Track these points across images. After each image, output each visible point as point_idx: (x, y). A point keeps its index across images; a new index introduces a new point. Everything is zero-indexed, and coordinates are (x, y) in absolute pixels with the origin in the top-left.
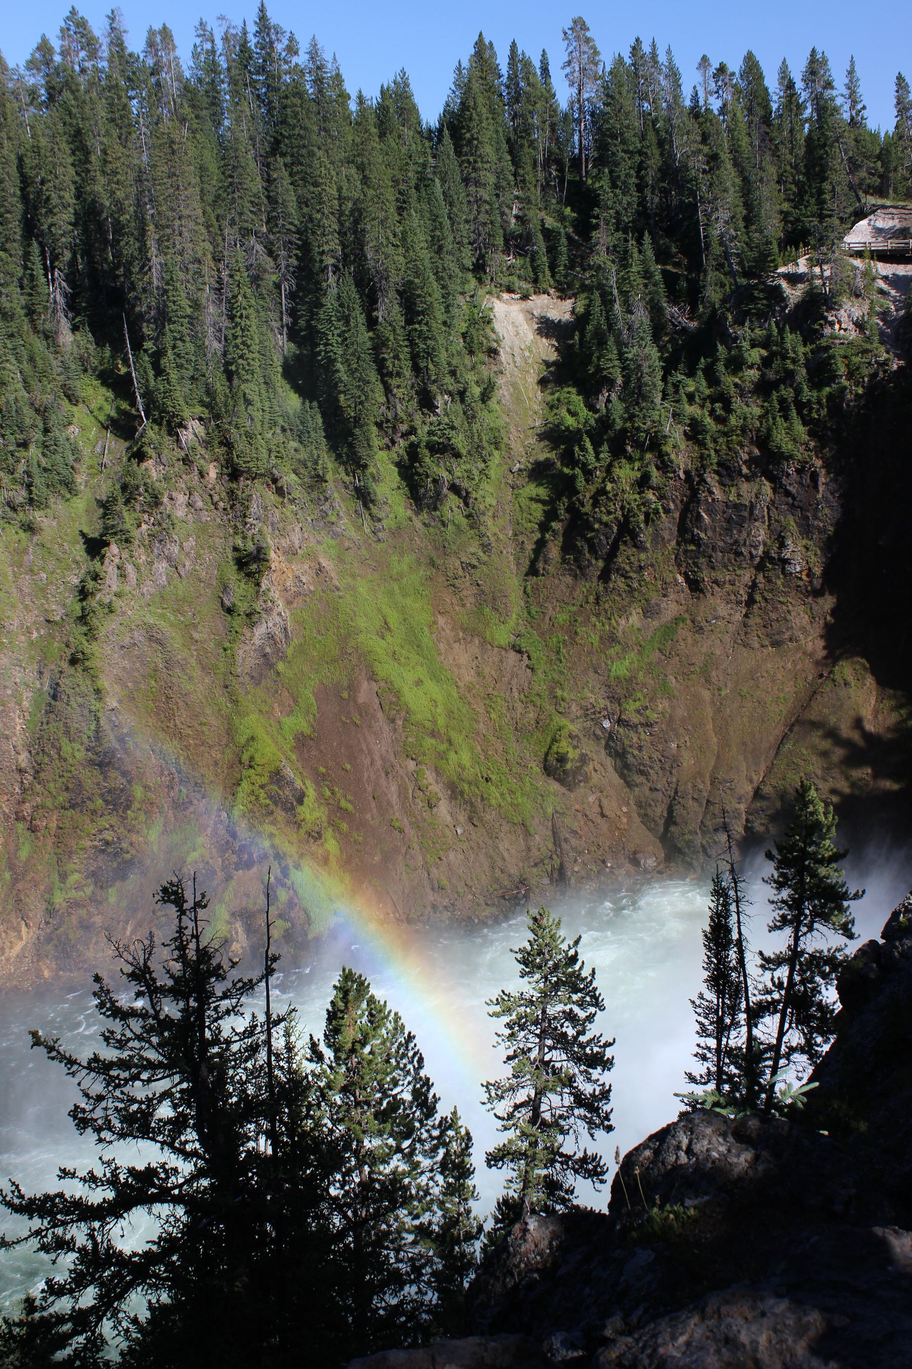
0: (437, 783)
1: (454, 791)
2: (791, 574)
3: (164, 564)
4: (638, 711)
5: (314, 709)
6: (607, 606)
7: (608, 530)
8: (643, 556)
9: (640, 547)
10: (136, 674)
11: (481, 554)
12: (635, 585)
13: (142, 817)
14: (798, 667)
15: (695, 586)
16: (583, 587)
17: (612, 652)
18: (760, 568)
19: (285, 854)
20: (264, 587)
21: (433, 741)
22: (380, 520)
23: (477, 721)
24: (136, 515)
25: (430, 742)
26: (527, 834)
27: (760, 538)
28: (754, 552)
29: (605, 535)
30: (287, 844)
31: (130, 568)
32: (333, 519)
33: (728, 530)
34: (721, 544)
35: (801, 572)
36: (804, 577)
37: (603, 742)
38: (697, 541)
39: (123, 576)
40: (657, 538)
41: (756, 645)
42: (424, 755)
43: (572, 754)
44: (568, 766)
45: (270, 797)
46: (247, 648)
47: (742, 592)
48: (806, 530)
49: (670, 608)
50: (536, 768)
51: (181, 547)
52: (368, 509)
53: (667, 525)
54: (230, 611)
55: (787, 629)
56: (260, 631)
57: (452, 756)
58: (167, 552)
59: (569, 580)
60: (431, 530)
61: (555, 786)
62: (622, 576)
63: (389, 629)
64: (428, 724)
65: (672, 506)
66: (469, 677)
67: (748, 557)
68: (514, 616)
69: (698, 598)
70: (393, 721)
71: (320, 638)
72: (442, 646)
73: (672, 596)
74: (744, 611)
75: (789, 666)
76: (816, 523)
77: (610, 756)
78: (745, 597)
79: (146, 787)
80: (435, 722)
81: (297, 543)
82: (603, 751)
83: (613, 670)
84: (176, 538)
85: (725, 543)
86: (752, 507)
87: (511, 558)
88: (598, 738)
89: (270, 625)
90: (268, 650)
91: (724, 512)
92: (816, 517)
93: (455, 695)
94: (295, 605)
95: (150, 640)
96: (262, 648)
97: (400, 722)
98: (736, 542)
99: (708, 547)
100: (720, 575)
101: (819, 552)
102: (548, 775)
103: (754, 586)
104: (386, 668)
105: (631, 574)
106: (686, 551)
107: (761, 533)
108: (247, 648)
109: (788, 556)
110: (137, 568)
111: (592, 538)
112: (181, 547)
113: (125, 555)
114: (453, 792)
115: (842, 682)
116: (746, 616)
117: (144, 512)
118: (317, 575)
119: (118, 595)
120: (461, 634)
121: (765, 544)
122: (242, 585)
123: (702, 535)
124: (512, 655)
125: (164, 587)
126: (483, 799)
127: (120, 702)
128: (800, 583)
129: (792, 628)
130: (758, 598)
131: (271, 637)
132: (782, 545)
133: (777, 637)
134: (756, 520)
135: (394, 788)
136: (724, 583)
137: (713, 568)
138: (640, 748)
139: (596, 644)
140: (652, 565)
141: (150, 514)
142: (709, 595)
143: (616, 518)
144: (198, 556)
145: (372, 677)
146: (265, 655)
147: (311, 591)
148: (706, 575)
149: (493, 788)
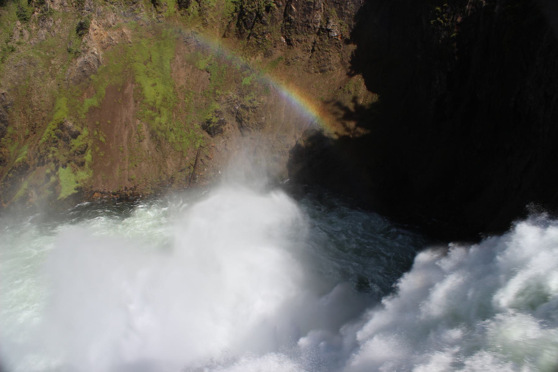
0: (147, 130)
1: (153, 134)
2: (332, 37)
3: (45, 31)
4: (250, 101)
5: (103, 96)
6: (246, 51)
7: (251, 15)
8: (265, 28)
9: (264, 23)
10: (20, 78)
11: (202, 28)
12: (260, 42)
13: (9, 141)
14: (331, 83)
15: (289, 42)
16: (241, 42)
17: (245, 73)
18: (318, 34)
19: (58, 161)
20: (84, 41)
21: (150, 112)
22: (160, 13)
23: (178, 104)
24: (32, 8)
25: (149, 112)
26: (182, 157)
27: (318, 19)
28: (316, 26)
29: (250, 18)
30: (61, 156)
31: (25, 32)
32: (137, 12)
33: (304, 15)
34: (301, 22)
35: (337, 36)
36: (339, 39)
37: (235, 115)
38: (289, 20)
39: (22, 35)
40: (273, 19)
41: (313, 72)
42: (144, 117)
43: (215, 120)
44: (211, 126)
45: (57, 135)
46: (73, 68)
47: (310, 46)
48: (341, 15)
49: (278, 53)
50: (197, 126)
51: (54, 23)
52: (156, 7)
53: (278, 12)
54: (69, 51)
55: (328, 64)
56: (80, 60)
57: (157, 119)
58: (46, 25)
59: (236, 39)
60: (184, 17)
61: (206, 134)
62: (255, 37)
63: (151, 61)
64: (151, 104)
65: (281, 3)
66: (183, 83)
67: (313, 28)
68: (210, 56)
69: (290, 48)
70: (136, 102)
71: (115, 64)
72: (174, 69)
73: (278, 47)
74: (310, 55)
75: (327, 82)
76: (346, 11)
77: (237, 121)
78: (311, 48)
79: (15, 128)
80: (154, 103)
81: (111, 22)
82: (235, 119)
83: (244, 81)
84: (52, 19)
85: (303, 21)
86: (315, 3)
87: (218, 30)
88: (233, 113)
89: (86, 58)
90: (85, 69)
91: (303, 6)
92: (346, 9)
93: (171, 91)
94: (107, 50)
95: (30, 63)
96: (81, 68)
97: (139, 103)
98: (308, 21)
99: (295, 23)
100: (300, 38)
101: (348, 27)
102: (204, 129)
103: (315, 43)
104: (141, 79)
105: (258, 36)
106: (285, 25)
107: (319, 17)
108: (73, 68)
109: (330, 28)
110: (30, 32)
111: (245, 20)
112: (54, 23)
113: (24, 26)
114: (152, 135)
115: (347, 92)
116: (310, 57)
117: (36, 7)
118: (121, 36)
119: (19, 44)
120: (185, 64)
121: (321, 22)
122: (77, 40)
123: (292, 18)
124: (205, 73)
125: (43, 40)
126: (166, 139)
127: (9, 90)
128: (337, 42)
129: (331, 63)
130: (316, 48)
131: (87, 63)
132: (328, 23)
133: (323, 68)
134: (317, 10)
135: (127, 132)
136: (302, 41)
137: (297, 34)
138: (248, 119)
139: (239, 69)
140: (270, 33)
141: (38, 8)
142: (295, 47)
143: (255, 10)
144: (62, 27)
145: (133, 82)
146: (84, 71)
147: (116, 44)
148: (293, 38)
149: (172, 134)
